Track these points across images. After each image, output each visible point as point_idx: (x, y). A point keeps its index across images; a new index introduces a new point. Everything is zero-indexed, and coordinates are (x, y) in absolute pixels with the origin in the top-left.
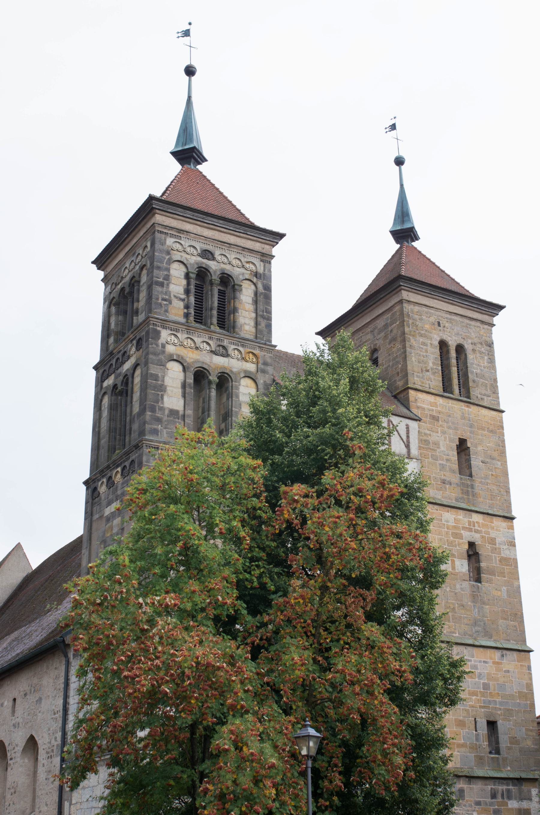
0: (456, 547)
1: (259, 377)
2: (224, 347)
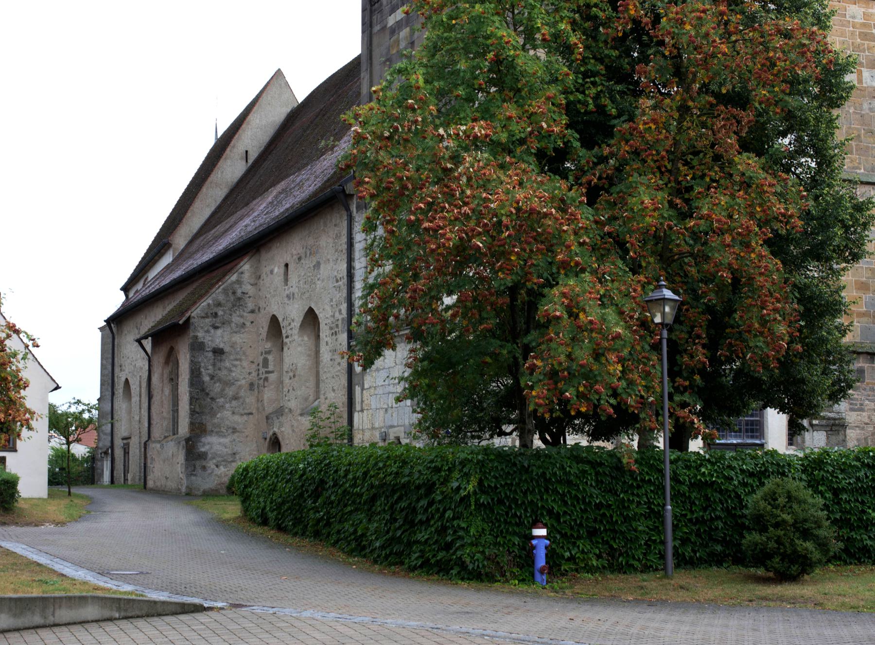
0: (864, 52)
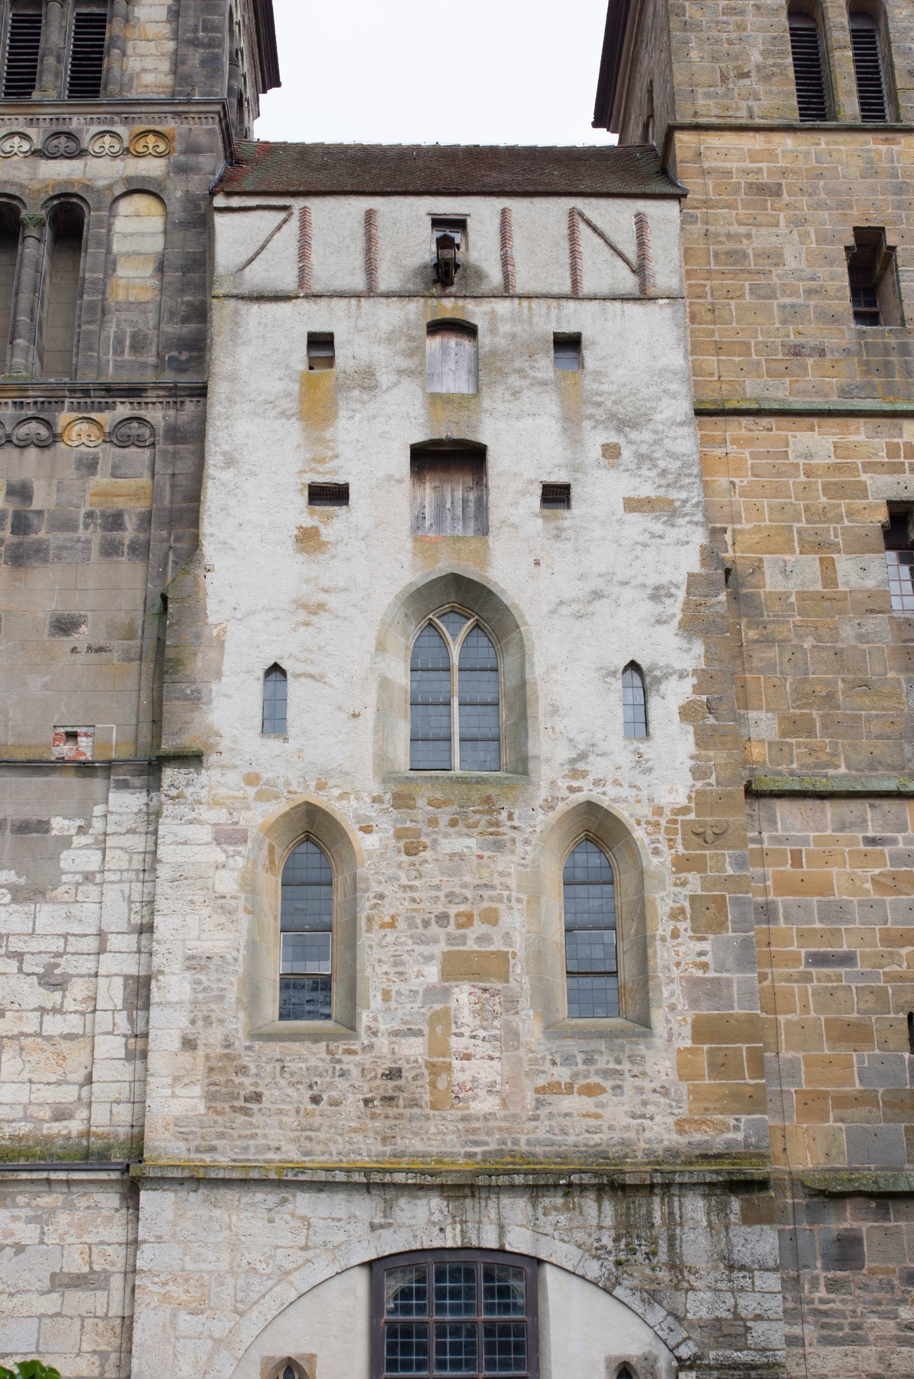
0: (839, 519)
1: (170, 186)
2: (70, 135)
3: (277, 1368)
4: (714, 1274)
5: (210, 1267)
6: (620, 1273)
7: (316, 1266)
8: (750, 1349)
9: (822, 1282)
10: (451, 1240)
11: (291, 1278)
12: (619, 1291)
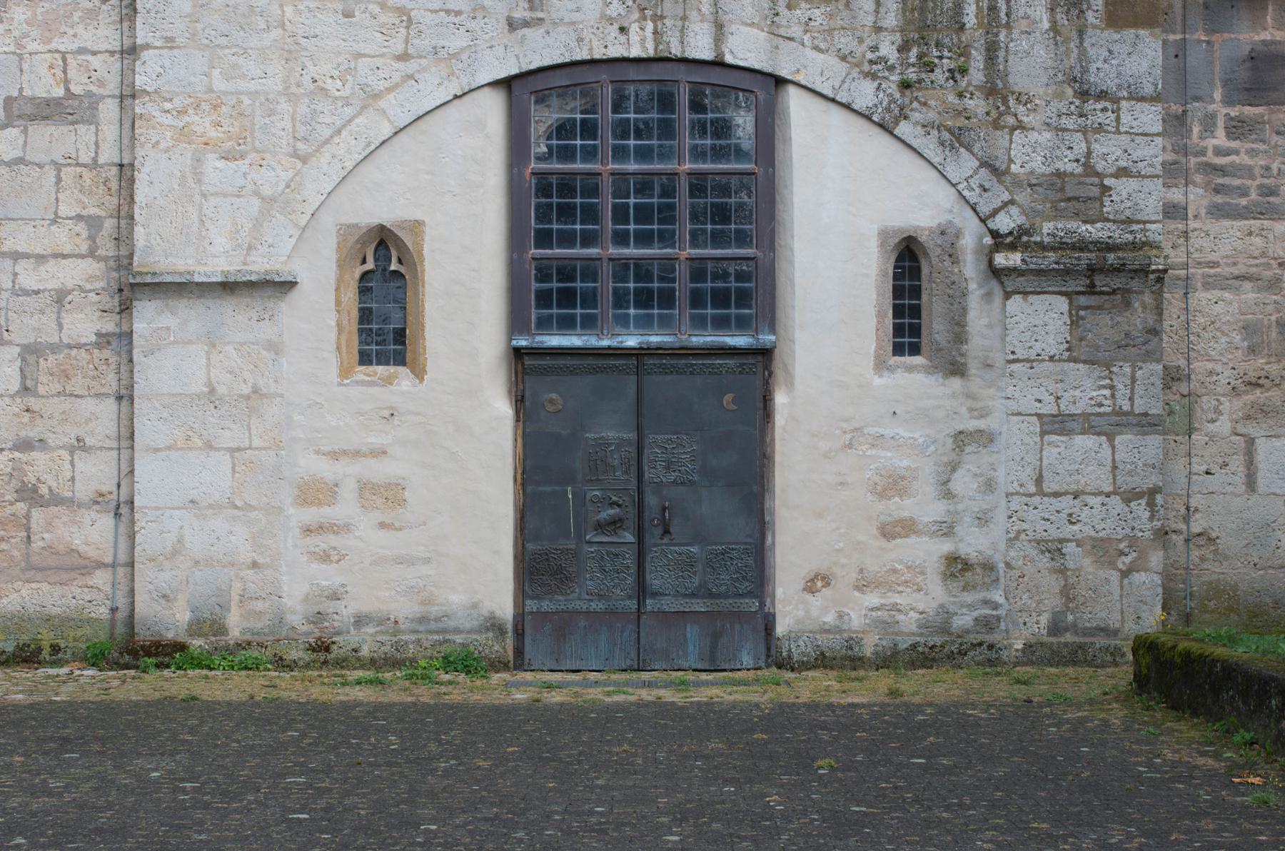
3: (363, 241)
4: (1055, 104)
5: (252, 86)
6: (907, 101)
7: (421, 86)
8: (1108, 220)
9: (1221, 123)
10: (638, 45)
11: (382, 104)
12: (903, 129)
